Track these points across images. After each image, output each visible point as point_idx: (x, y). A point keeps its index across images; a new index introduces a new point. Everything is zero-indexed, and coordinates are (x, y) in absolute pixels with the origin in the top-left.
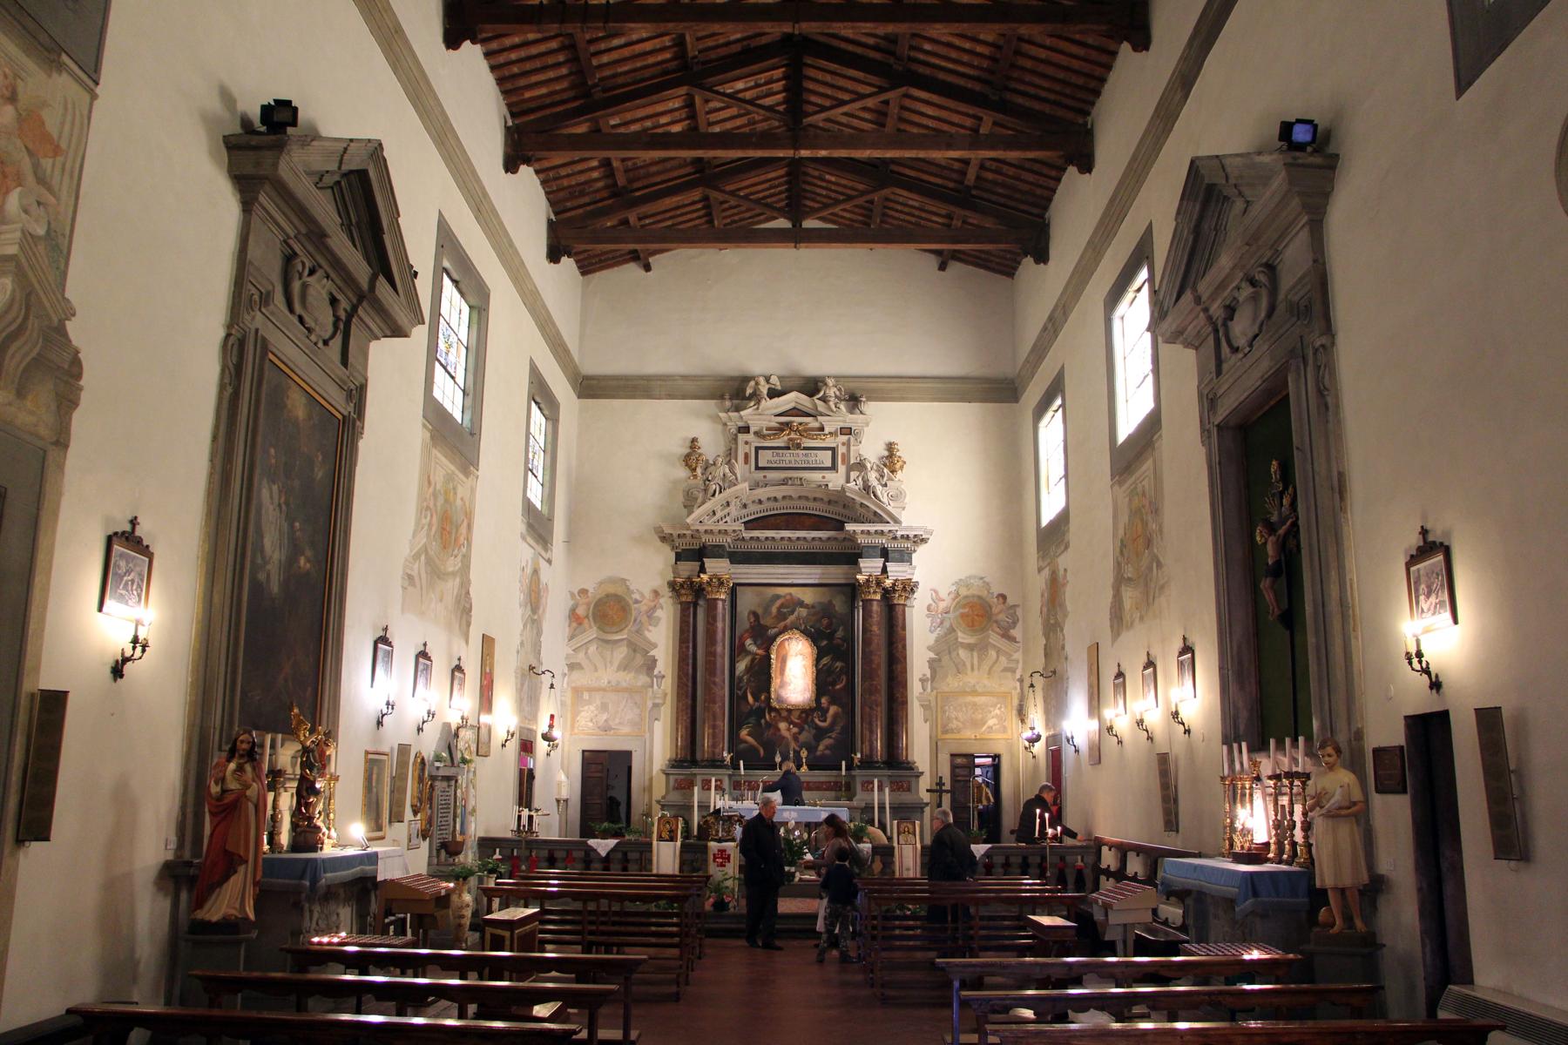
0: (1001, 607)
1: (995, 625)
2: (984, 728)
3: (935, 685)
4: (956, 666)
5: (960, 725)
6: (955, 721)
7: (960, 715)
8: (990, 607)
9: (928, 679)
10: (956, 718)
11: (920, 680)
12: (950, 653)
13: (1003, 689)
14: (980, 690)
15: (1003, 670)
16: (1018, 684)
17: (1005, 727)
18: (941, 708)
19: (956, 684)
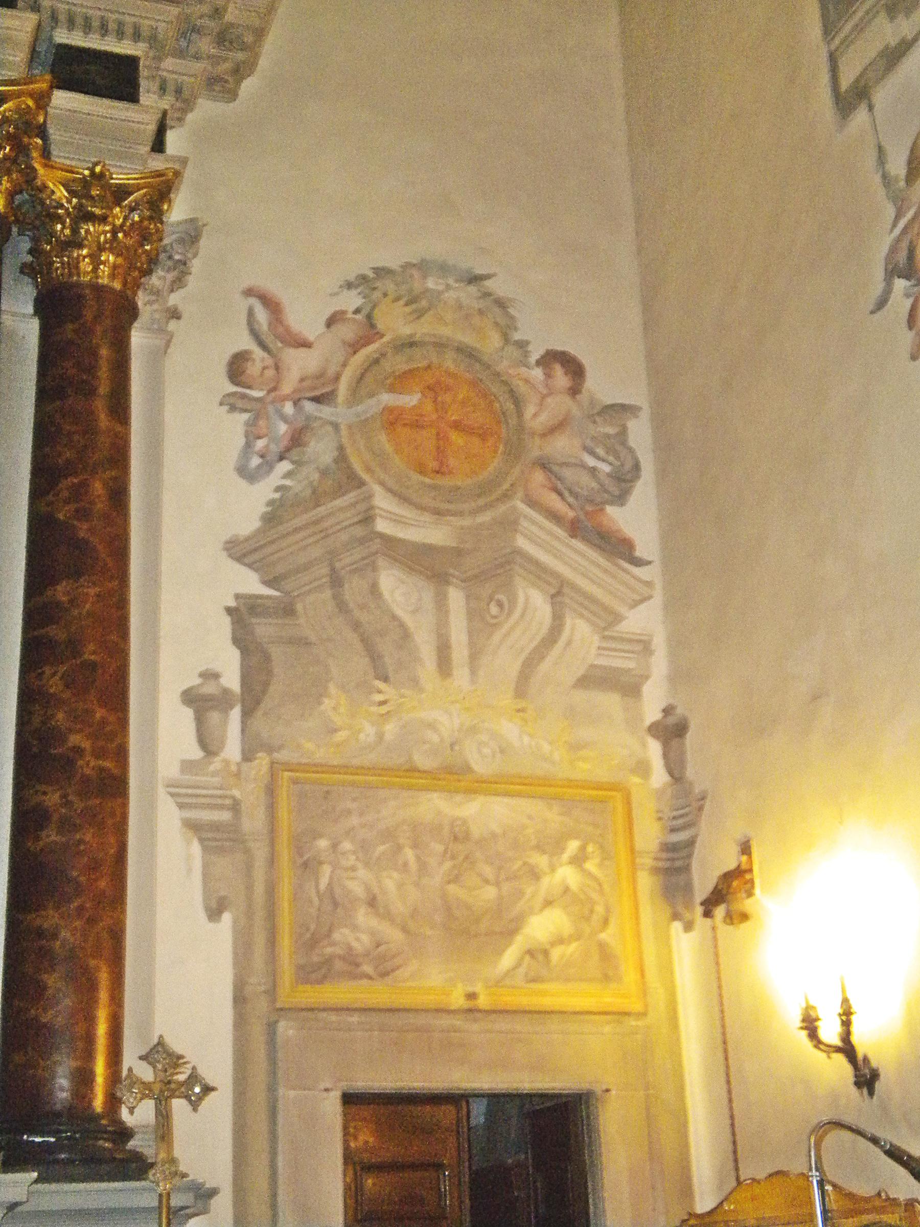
0: (559, 404)
1: (539, 477)
2: (508, 958)
3: (258, 723)
4: (365, 640)
5: (394, 935)
6: (362, 916)
7: (390, 882)
8: (517, 401)
9: (223, 700)
10: (372, 902)
11: (190, 698)
12: (336, 581)
13: (585, 769)
14: (480, 767)
15: (587, 681)
16: (654, 749)
17: (606, 954)
18: (299, 844)
19: (368, 732)
